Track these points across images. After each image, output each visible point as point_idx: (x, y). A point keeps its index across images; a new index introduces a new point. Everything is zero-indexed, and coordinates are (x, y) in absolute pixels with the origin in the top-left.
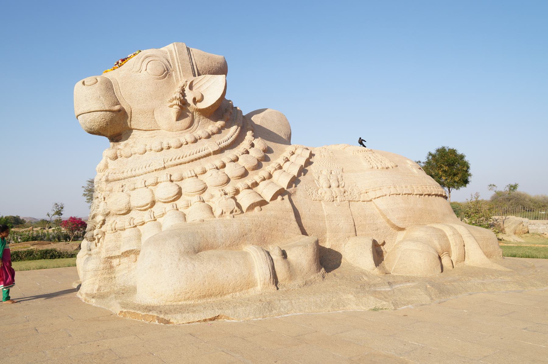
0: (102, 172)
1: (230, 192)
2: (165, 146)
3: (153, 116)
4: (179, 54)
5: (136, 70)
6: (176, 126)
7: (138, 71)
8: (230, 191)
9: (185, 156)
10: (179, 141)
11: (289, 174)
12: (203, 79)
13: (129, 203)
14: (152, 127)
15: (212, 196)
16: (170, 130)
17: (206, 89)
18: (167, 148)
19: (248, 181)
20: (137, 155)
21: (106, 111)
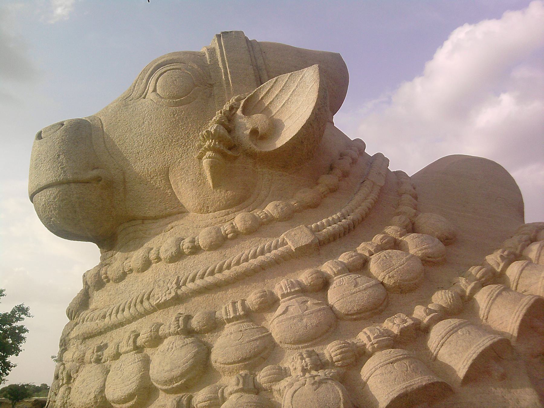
0: (74, 319)
1: (334, 359)
2: (186, 245)
3: (168, 183)
4: (227, 52)
5: (138, 95)
6: (214, 198)
7: (141, 96)
8: (332, 355)
9: (225, 266)
10: (218, 231)
11: (522, 295)
12: (272, 87)
13: (102, 390)
14: (166, 209)
15: (282, 374)
16: (204, 209)
17: (282, 107)
18: (189, 250)
19: (391, 324)
20: (134, 274)
21: (69, 182)
